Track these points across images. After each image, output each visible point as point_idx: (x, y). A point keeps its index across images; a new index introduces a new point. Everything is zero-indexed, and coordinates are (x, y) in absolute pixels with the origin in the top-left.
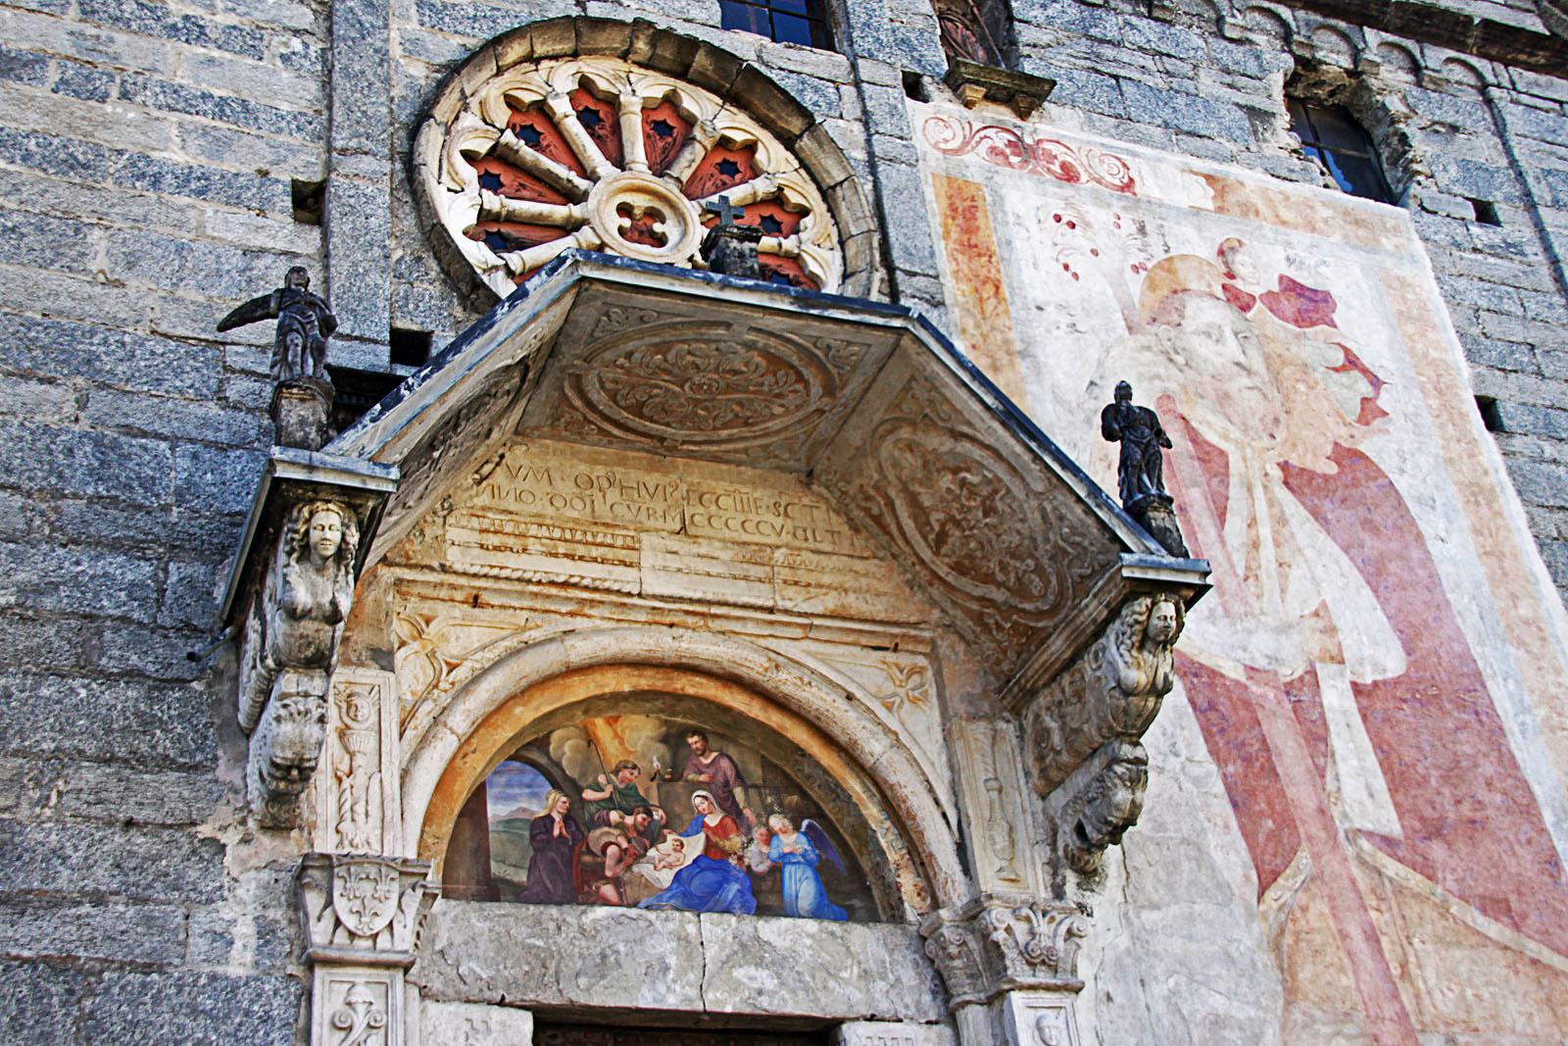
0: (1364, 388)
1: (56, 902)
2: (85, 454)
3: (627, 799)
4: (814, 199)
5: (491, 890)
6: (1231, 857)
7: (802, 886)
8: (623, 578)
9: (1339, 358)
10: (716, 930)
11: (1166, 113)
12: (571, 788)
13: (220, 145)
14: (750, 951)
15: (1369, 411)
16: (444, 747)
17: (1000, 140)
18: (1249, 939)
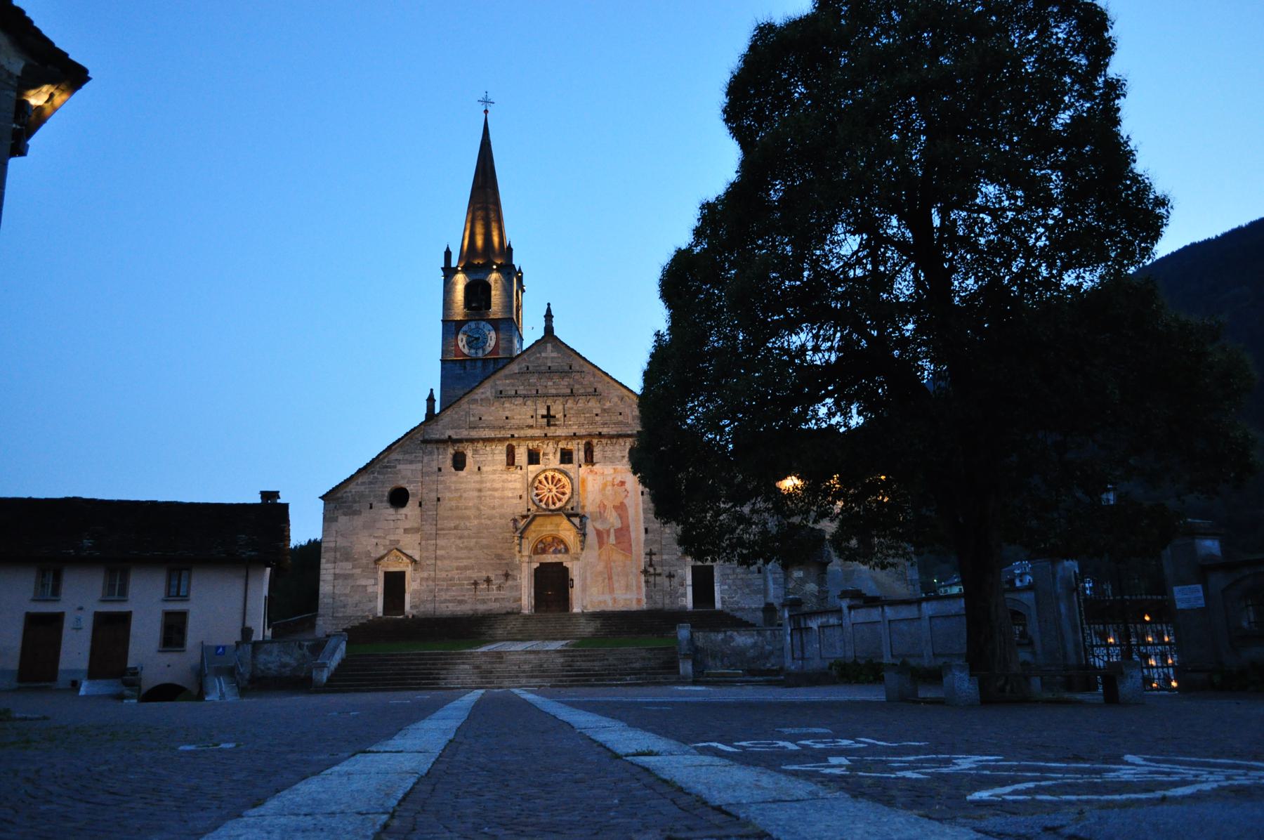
3: (549, 544)
5: (538, 554)
6: (596, 547)
7: (563, 550)
10: (553, 556)
13: (513, 493)
14: (556, 557)
15: (626, 496)
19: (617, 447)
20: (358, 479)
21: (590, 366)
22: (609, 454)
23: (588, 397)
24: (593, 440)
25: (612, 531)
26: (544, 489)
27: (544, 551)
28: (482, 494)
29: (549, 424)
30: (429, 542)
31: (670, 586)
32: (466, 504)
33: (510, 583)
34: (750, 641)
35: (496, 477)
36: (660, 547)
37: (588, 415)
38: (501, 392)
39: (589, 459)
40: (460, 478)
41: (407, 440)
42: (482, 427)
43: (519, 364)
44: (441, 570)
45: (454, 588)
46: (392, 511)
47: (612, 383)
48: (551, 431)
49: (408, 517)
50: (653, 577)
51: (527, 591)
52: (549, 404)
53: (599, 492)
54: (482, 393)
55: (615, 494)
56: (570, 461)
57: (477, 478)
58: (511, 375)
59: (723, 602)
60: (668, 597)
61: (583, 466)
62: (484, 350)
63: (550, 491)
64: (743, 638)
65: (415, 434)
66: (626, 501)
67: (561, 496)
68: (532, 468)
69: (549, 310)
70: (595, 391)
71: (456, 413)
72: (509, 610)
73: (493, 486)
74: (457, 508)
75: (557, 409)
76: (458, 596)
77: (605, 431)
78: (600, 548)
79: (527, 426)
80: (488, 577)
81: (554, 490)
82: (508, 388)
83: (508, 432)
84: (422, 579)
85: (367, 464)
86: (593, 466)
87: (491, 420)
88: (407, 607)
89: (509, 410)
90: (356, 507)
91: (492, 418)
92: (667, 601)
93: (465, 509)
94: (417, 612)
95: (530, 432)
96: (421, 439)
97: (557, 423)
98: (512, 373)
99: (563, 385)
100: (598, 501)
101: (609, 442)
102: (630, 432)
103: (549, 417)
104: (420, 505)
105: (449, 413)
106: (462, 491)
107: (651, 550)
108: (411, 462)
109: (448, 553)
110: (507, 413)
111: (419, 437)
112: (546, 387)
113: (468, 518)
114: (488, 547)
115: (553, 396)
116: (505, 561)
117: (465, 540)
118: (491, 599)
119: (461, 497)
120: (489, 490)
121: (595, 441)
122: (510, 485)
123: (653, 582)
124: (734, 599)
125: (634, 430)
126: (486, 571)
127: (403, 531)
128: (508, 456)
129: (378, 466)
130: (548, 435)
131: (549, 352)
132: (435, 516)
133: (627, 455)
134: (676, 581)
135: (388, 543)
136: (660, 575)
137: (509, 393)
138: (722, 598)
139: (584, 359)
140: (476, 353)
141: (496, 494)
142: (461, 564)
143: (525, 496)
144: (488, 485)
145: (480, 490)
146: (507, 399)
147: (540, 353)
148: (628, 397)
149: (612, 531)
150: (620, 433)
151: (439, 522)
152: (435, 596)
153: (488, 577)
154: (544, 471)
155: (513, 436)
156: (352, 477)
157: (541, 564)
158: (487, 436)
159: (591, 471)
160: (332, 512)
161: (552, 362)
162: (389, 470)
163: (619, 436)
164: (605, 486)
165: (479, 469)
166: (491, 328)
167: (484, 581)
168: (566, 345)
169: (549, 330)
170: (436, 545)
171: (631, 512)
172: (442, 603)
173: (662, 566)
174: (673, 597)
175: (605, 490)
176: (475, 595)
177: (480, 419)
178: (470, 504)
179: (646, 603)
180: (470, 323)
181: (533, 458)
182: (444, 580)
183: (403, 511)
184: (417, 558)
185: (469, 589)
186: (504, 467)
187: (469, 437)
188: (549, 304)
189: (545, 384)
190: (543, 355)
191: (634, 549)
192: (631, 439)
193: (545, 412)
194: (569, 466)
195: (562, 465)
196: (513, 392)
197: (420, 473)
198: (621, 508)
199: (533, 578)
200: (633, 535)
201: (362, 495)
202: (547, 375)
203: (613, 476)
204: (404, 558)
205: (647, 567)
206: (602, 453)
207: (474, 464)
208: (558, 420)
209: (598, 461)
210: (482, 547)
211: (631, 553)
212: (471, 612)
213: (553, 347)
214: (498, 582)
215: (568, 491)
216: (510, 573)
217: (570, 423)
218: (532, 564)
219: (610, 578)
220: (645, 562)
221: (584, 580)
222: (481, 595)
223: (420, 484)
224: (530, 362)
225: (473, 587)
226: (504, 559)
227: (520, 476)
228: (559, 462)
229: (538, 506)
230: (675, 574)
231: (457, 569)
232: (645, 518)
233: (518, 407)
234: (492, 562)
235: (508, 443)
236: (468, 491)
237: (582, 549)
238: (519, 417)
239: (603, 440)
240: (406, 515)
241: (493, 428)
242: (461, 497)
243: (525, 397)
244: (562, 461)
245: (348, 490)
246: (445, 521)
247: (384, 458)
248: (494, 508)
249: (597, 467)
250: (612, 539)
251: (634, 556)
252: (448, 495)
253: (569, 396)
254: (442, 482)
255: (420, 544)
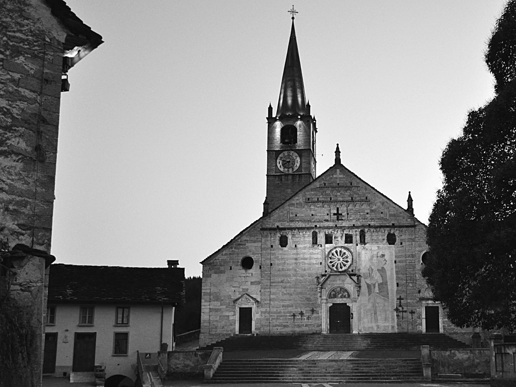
0: (385, 262)
1: (312, 301)
2: (312, 281)
3: (338, 292)
4: (349, 256)
5: (331, 298)
7: (347, 296)
8: (336, 283)
9: (384, 260)
10: (341, 299)
11: (376, 241)
12: (335, 292)
13: (316, 261)
14: (343, 300)
16: (328, 292)
17: (362, 248)
18: (367, 299)
19: (380, 233)
20: (222, 252)
21: (363, 183)
22: (375, 238)
23: (362, 203)
24: (365, 229)
25: (377, 285)
26: (335, 259)
27: (335, 296)
28: (298, 261)
29: (338, 219)
30: (266, 290)
31: (412, 318)
32: (288, 268)
33: (315, 315)
34: (466, 356)
35: (305, 251)
36: (406, 295)
37: (362, 214)
38: (309, 199)
39: (363, 241)
40: (285, 252)
41: (252, 228)
42: (298, 221)
43: (320, 182)
44: (273, 307)
45: (281, 318)
46: (243, 271)
47: (377, 193)
48: (339, 224)
49: (253, 275)
50: (401, 313)
51: (325, 321)
52: (338, 207)
53: (369, 261)
54: (297, 200)
55: (379, 262)
56: (351, 242)
57: (295, 251)
58: (315, 188)
59: (444, 329)
60: (411, 325)
61: (359, 245)
62: (293, 169)
63: (339, 260)
64: (462, 355)
65: (257, 224)
66: (385, 267)
67: (346, 263)
68: (327, 245)
69: (338, 148)
70: (366, 197)
71: (282, 212)
72: (314, 332)
73: (304, 257)
74: (283, 269)
75: (343, 210)
76: (284, 323)
77: (372, 223)
78: (369, 295)
79: (325, 220)
80: (301, 311)
81: (341, 259)
82: (313, 197)
83: (313, 224)
84: (262, 312)
85: (228, 243)
86: (365, 245)
87: (303, 216)
88: (253, 329)
89: (314, 210)
90: (222, 268)
91: (303, 215)
92: (410, 328)
93: (287, 271)
94: (259, 332)
95: (326, 224)
96: (261, 228)
97: (343, 218)
98: (315, 187)
99: (347, 195)
100: (368, 266)
101: (375, 230)
102: (387, 224)
103: (338, 214)
104: (260, 268)
105: (277, 212)
106: (285, 259)
107: (400, 296)
108: (255, 242)
109: (277, 297)
110: (313, 212)
111: (259, 226)
112: (336, 196)
113: (289, 276)
114: (301, 293)
115: (341, 202)
116: (312, 302)
117: (288, 289)
118: (303, 325)
119: (285, 263)
120: (302, 259)
121: (366, 230)
122: (315, 256)
123: (401, 316)
124: (451, 327)
125: (390, 223)
126: (300, 308)
127: (250, 283)
128: (313, 238)
129: (235, 244)
130: (338, 226)
131: (338, 175)
132: (269, 274)
133: (386, 239)
134: (415, 316)
135: (241, 290)
136: (406, 311)
137: (314, 200)
138: (444, 326)
139: (360, 179)
140: (288, 171)
141: (306, 261)
142: (284, 304)
143: (323, 263)
144: (301, 256)
145: (296, 259)
146: (312, 203)
147: (332, 175)
148: (387, 202)
149: (377, 285)
150: (381, 225)
151: (272, 278)
152: (270, 323)
153: (301, 311)
154: (335, 248)
155: (316, 226)
156: (219, 250)
157: (333, 304)
158: (301, 226)
159: (364, 248)
160: (207, 271)
161: (340, 181)
162: (241, 246)
163: (381, 227)
164: (372, 257)
165: (296, 246)
166: (297, 155)
167: (299, 314)
168: (349, 170)
169: (338, 160)
170: (270, 292)
171: (388, 273)
172: (274, 327)
173: (407, 306)
174: (414, 325)
175: (372, 260)
176: (294, 322)
177: (296, 215)
178: (290, 268)
179: (398, 329)
180: (284, 152)
181: (329, 240)
182: (275, 313)
183: (250, 271)
184: (259, 300)
185: (290, 318)
186: (311, 245)
187: (289, 226)
188: (338, 145)
189: (335, 194)
190: (334, 176)
191: (390, 296)
192: (388, 229)
193: (336, 212)
194: (351, 244)
195: (346, 244)
196: (316, 199)
197: (260, 248)
198: (382, 271)
199: (329, 312)
200: (389, 288)
201: (225, 262)
202: (337, 188)
203: (377, 251)
204: (251, 300)
205: (398, 307)
206: (370, 237)
207: (293, 243)
208: (344, 216)
209: (369, 242)
210: (298, 294)
211: (388, 299)
212: (291, 333)
213: (340, 171)
214: (308, 314)
215: (350, 260)
216: (315, 309)
217: (351, 218)
218: (328, 304)
219: (375, 313)
220: (396, 304)
221: (360, 314)
222: (298, 322)
223: (260, 255)
224: (326, 180)
225: (293, 317)
226: (311, 301)
227: (320, 251)
228: (344, 242)
229: (331, 269)
230: (415, 311)
231: (283, 307)
232: (397, 277)
233: (319, 208)
234: (304, 302)
235: (313, 230)
236: (289, 260)
237: (358, 296)
238: (320, 214)
239: (371, 229)
240: (252, 274)
241: (304, 221)
242: (285, 263)
243: (323, 202)
244: (346, 242)
245: (217, 258)
246: (276, 278)
247: (238, 239)
248: (305, 270)
249: (367, 246)
250: (377, 290)
251: (390, 301)
252: (277, 262)
253: (350, 202)
254: (274, 254)
255: (260, 291)
